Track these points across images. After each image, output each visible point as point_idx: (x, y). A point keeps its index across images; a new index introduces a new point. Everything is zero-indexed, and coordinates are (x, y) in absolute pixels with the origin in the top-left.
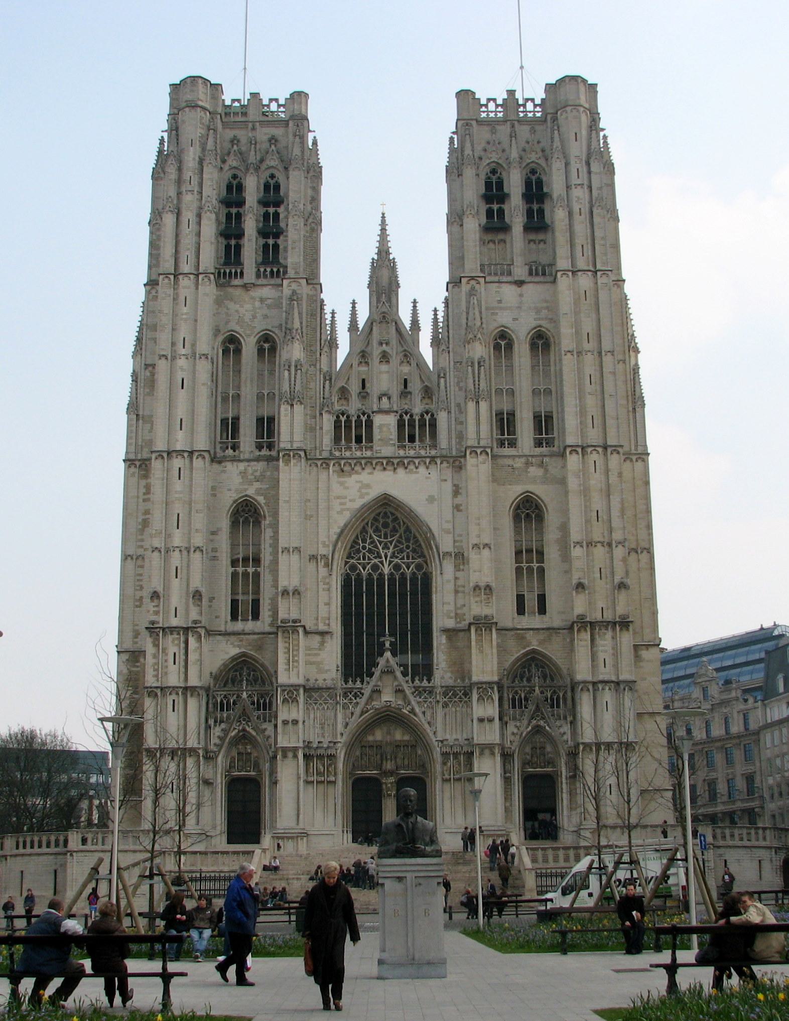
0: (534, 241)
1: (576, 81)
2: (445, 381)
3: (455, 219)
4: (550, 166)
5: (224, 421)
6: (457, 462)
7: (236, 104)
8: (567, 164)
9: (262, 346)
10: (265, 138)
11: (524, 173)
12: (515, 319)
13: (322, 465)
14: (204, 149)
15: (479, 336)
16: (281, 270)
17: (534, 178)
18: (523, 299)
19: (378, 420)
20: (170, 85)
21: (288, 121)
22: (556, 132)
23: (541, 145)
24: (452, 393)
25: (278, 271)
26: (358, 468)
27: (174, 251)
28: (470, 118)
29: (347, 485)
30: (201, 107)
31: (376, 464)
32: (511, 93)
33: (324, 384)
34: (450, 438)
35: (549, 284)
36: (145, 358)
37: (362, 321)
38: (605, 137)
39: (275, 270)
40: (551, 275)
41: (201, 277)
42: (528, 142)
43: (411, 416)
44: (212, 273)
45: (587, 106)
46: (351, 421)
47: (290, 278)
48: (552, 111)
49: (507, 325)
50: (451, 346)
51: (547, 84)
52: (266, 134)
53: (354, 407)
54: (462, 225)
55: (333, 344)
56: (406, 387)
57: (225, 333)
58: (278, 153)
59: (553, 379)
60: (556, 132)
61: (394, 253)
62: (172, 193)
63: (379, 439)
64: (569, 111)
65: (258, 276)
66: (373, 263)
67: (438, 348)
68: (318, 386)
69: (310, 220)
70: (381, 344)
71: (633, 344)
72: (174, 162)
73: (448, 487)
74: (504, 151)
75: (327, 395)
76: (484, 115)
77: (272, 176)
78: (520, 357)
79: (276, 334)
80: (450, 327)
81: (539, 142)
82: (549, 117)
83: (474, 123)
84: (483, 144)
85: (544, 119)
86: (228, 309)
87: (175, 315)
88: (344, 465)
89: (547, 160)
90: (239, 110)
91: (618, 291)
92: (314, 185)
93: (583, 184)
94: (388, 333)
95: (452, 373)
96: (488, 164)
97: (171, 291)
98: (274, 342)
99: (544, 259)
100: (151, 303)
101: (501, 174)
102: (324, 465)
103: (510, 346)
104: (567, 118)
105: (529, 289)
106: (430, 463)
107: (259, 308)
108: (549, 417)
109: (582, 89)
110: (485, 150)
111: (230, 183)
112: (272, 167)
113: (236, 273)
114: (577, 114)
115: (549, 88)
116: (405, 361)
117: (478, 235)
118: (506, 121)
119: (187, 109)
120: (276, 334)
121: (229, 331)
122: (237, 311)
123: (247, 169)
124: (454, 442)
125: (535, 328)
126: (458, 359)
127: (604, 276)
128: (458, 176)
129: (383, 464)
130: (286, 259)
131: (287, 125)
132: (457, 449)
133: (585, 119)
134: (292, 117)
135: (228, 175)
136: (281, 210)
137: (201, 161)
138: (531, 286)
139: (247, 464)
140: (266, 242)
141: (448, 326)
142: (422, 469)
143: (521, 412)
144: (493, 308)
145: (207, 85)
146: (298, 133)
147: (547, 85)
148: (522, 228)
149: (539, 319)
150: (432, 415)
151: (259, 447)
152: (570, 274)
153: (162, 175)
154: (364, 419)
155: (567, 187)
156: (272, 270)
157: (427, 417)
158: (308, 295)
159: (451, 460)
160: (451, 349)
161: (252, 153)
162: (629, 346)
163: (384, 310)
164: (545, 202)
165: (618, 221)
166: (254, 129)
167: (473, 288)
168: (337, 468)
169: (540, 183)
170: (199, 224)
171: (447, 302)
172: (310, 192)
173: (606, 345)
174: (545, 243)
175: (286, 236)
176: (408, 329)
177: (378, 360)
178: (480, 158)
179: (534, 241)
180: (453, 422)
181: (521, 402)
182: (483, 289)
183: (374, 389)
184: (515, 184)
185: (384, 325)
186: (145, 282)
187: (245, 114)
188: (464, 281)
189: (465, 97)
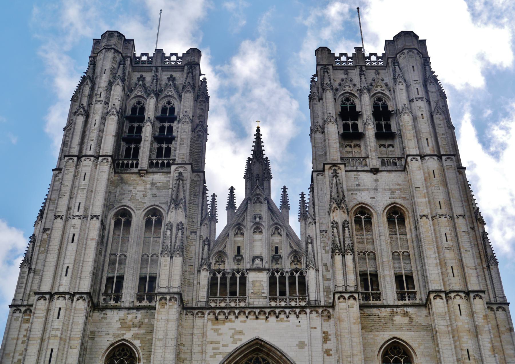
0: (384, 146)
7: (144, 58)
9: (150, 219)
11: (372, 99)
13: (197, 314)
15: (343, 205)
18: (378, 183)
19: (251, 277)
22: (397, 67)
23: (385, 82)
24: (319, 254)
26: (232, 317)
27: (80, 141)
29: (220, 332)
31: (249, 313)
33: (203, 247)
34: (318, 292)
35: (400, 173)
36: (45, 224)
41: (100, 159)
43: (282, 274)
44: (110, 156)
46: (226, 278)
47: (177, 164)
49: (365, 202)
52: (166, 75)
53: (229, 265)
54: (323, 132)
55: (213, 218)
57: (118, 207)
58: (174, 87)
59: (410, 244)
60: (397, 67)
63: (253, 293)
65: (151, 165)
67: (306, 222)
68: (197, 248)
69: (198, 129)
70: (255, 218)
71: (479, 217)
73: (318, 334)
74: (355, 85)
75: (205, 257)
76: (338, 64)
79: (163, 209)
80: (316, 204)
82: (390, 60)
83: (331, 67)
84: (338, 81)
86: (123, 190)
87: (73, 187)
88: (219, 314)
89: (390, 90)
91: (461, 177)
92: (202, 107)
94: (261, 211)
95: (318, 239)
96: (343, 94)
97: (73, 169)
98: (161, 215)
101: (353, 101)
102: (200, 314)
103: (369, 221)
105: (383, 176)
106: (300, 313)
107: (151, 189)
111: (135, 106)
112: (170, 96)
116: (276, 232)
118: (356, 66)
119: (104, 51)
120: (163, 209)
121: (121, 206)
122: (131, 191)
123: (149, 95)
124: (322, 295)
126: (324, 228)
128: (319, 101)
129: (255, 313)
131: (183, 70)
132: (325, 301)
135: (132, 102)
136: (175, 125)
138: (385, 173)
139: (127, 312)
140: (161, 146)
141: (314, 204)
142: (293, 317)
143: (383, 269)
144: (352, 190)
145: (121, 38)
147: (386, 41)
150: (301, 273)
151: (140, 298)
157: (297, 275)
159: (320, 310)
160: (317, 220)
163: (258, 191)
165: (454, 128)
166: (157, 71)
167: (335, 171)
168: (212, 316)
172: (199, 112)
174: (393, 147)
176: (279, 208)
177: (252, 231)
179: (382, 145)
180: (321, 278)
181: (383, 263)
182: (344, 176)
185: (258, 205)
186: (55, 167)
187: (151, 62)
188: (327, 167)
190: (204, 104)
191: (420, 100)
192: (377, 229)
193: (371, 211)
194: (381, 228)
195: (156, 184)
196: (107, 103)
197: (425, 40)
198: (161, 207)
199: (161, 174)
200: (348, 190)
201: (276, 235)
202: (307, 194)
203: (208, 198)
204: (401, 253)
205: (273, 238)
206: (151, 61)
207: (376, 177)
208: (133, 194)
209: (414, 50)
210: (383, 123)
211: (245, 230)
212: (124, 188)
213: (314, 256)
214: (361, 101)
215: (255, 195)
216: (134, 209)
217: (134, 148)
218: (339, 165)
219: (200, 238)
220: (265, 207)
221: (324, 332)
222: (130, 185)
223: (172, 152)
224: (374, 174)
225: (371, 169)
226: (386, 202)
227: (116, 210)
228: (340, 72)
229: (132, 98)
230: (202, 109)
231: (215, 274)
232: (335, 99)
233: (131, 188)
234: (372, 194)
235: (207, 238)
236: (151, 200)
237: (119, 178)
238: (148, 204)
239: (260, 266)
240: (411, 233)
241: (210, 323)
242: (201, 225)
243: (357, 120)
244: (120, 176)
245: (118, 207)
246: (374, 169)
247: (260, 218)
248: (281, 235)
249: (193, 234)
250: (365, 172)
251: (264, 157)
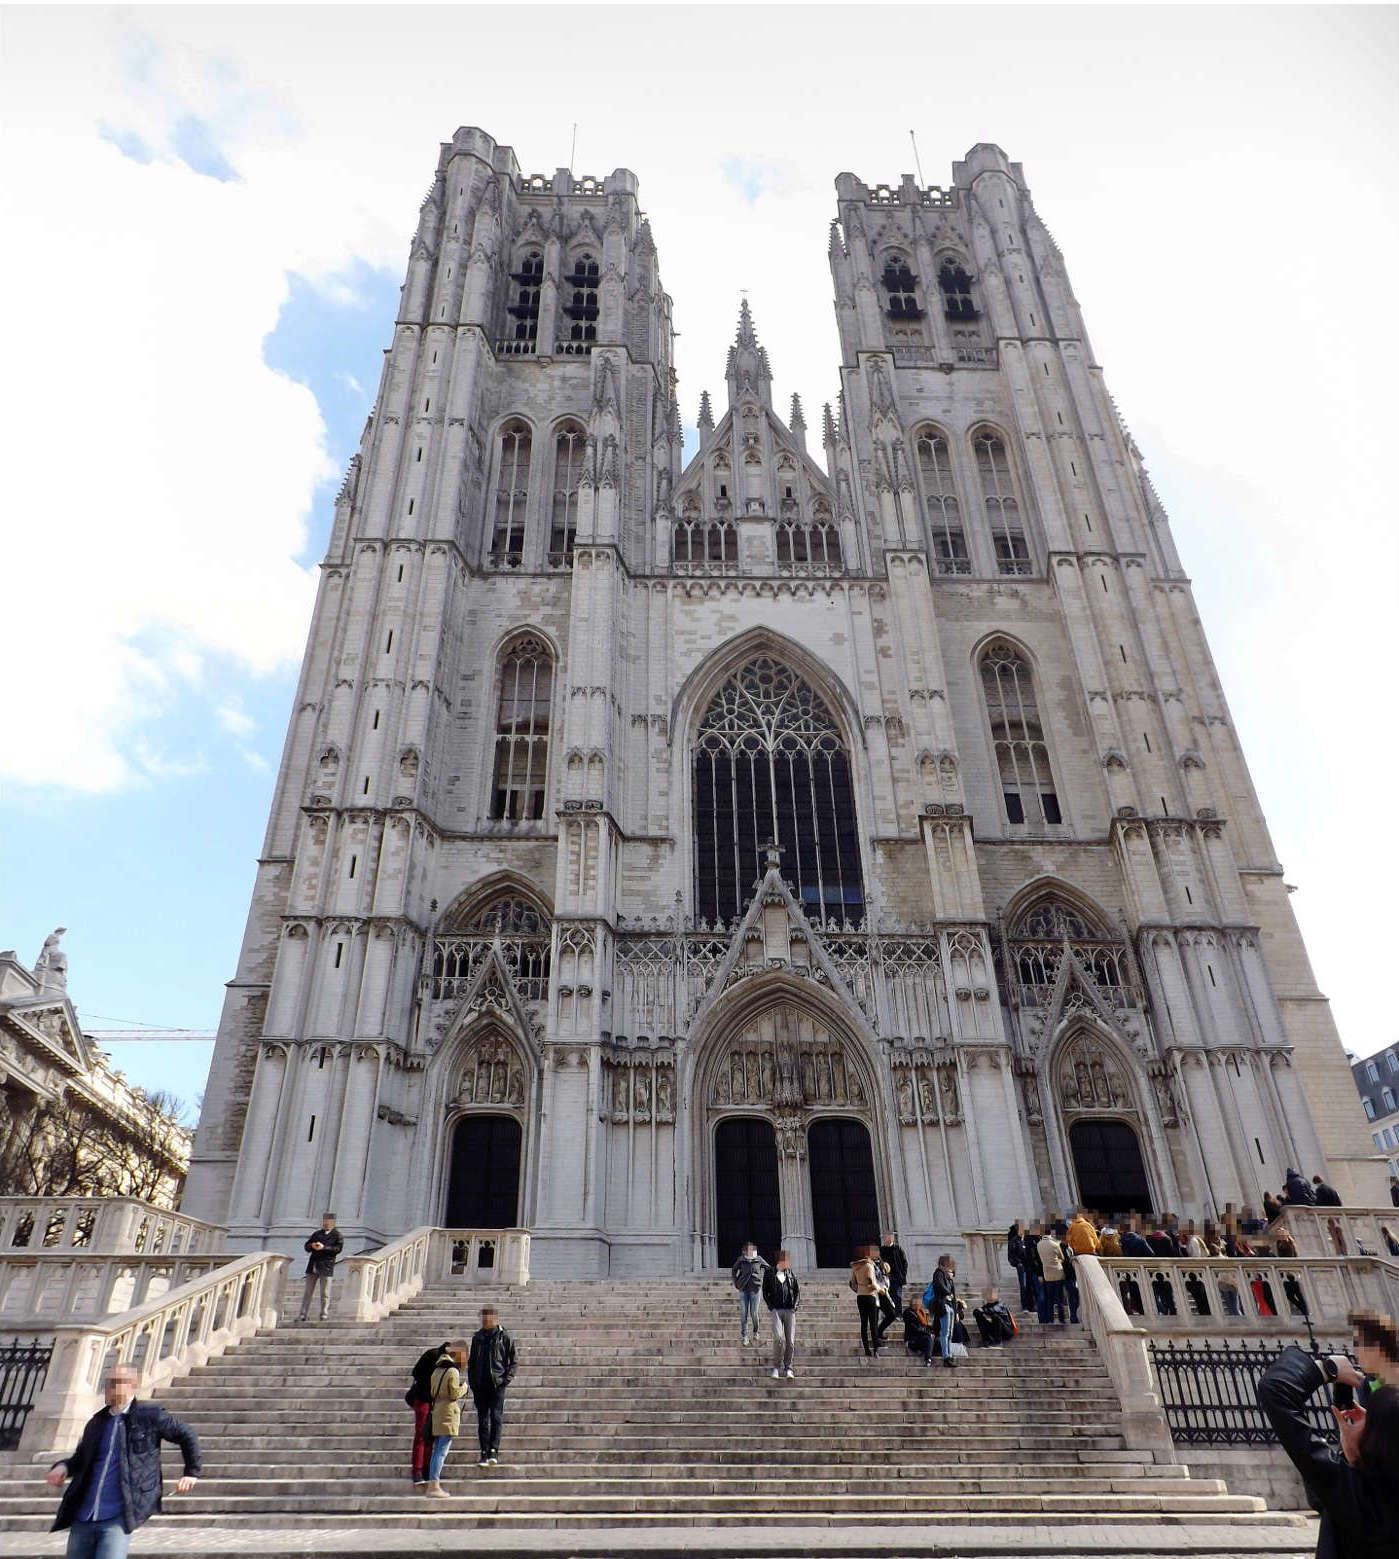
3: (845, 302)
5: (500, 533)
6: (877, 585)
7: (538, 183)
10: (577, 215)
12: (945, 411)
13: (654, 586)
19: (745, 531)
21: (607, 197)
24: (860, 498)
26: (714, 592)
29: (696, 615)
31: (744, 588)
32: (908, 178)
34: (861, 556)
43: (798, 527)
46: (702, 532)
53: (708, 513)
55: (673, 437)
59: (1016, 486)
61: (762, 340)
63: (748, 557)
65: (560, 350)
69: (637, 298)
73: (865, 622)
74: (906, 236)
83: (862, 204)
84: (876, 229)
88: (692, 587)
89: (967, 246)
103: (942, 448)
106: (832, 588)
122: (526, 390)
129: (754, 588)
138: (964, 372)
141: (846, 420)
142: (820, 596)
143: (971, 524)
149: (982, 412)
150: (831, 527)
154: (722, 529)
157: (823, 530)
159: (867, 585)
163: (748, 398)
166: (560, 203)
168: (679, 591)
171: (842, 397)
172: (638, 270)
177: (743, 459)
178: (875, 242)
179: (960, 332)
180: (865, 536)
181: (969, 513)
183: (736, 496)
184: (924, 266)
189: (845, 181)
194: (965, 459)
206: (550, 189)
214: (916, 259)
215: (745, 404)
220: (763, 421)
221: (876, 620)
222: (524, 381)
225: (941, 365)
228: (879, 214)
230: (644, 267)
232: (871, 255)
233: (527, 385)
235: (665, 469)
237: (504, 370)
238: (560, 412)
239: (759, 513)
241: (677, 602)
247: (756, 440)
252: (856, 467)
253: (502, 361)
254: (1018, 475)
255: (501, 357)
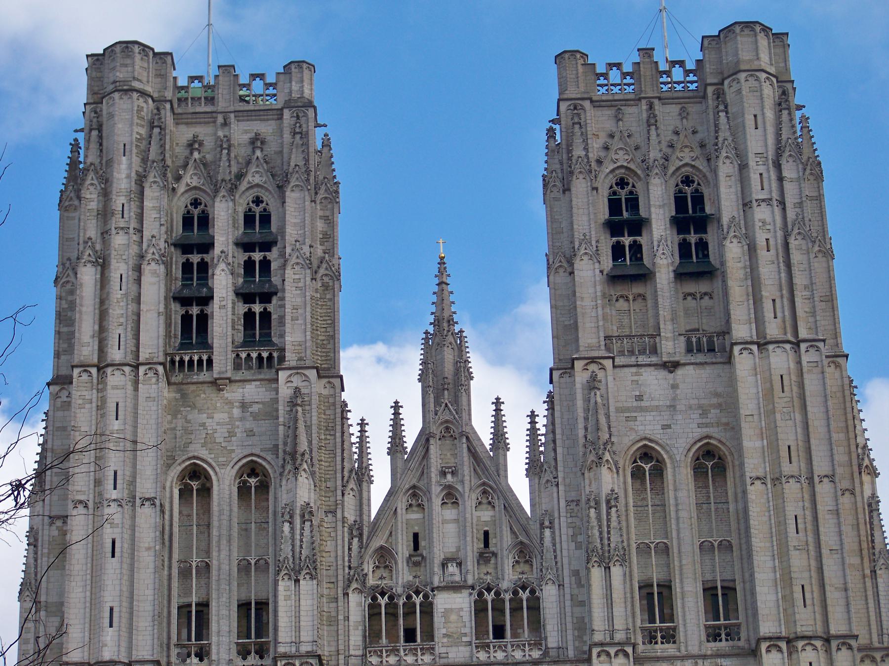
1: (753, 30)
2: (553, 533)
4: (715, 172)
8: (743, 167)
9: (245, 482)
10: (246, 137)
11: (672, 182)
14: (145, 160)
15: (607, 456)
16: (275, 355)
17: (688, 190)
18: (678, 392)
19: (442, 602)
20: (88, 56)
21: (282, 109)
22: (722, 114)
23: (699, 136)
24: (565, 553)
25: (270, 357)
27: (97, 327)
28: (579, 96)
30: (137, 91)
32: (647, 52)
33: (350, 544)
34: (563, 631)
35: (720, 366)
37: (411, 435)
38: (805, 119)
39: (265, 355)
40: (723, 349)
41: (142, 369)
42: (677, 133)
43: (498, 594)
44: (160, 364)
45: (772, 70)
46: (396, 606)
47: (290, 369)
48: (715, 81)
49: (652, 437)
50: (561, 475)
51: (703, 37)
52: (246, 132)
54: (572, 273)
56: (486, 544)
57: (184, 461)
60: (722, 114)
62: (92, 231)
63: (445, 635)
64: (742, 79)
65: (237, 366)
66: (426, 339)
68: (340, 548)
69: (322, 271)
70: (443, 474)
71: (866, 462)
72: (95, 182)
77: (258, 201)
78: (675, 490)
79: (269, 463)
80: (558, 442)
81: (694, 132)
82: (710, 90)
83: (587, 104)
84: (603, 139)
85: (702, 94)
86: (188, 422)
89: (709, 160)
90: (199, 93)
93: (771, 199)
96: (612, 171)
98: (266, 474)
99: (711, 325)
100: (60, 414)
101: (634, 186)
103: (659, 472)
104: (739, 91)
105: (686, 374)
107: (242, 419)
108: (729, 590)
109: (763, 42)
110: (607, 148)
112: (258, 185)
113: (200, 361)
114: (756, 84)
115: (710, 42)
116: (485, 501)
117: (599, 288)
118: (640, 99)
119: (116, 95)
120: (269, 463)
121: (189, 459)
122: (203, 425)
123: (216, 191)
124: (570, 637)
125: (700, 440)
126: (573, 495)
127: (812, 350)
128: (564, 192)
130: (282, 336)
131: (280, 117)
132: (576, 648)
133: (769, 92)
134: (289, 105)
135: (181, 203)
136: (273, 255)
137: (141, 180)
138: (691, 367)
141: (554, 441)
144: (628, 409)
145: (147, 55)
146: (298, 130)
148: (672, 275)
149: (707, 425)
150: (533, 592)
152: (755, 348)
153: (76, 202)
154: (418, 600)
155: (745, 205)
156: (260, 355)
157: (524, 595)
158: (320, 395)
160: (560, 480)
161: (224, 163)
162: (860, 466)
164: (709, 229)
166: (226, 124)
167: (594, 378)
169: (699, 199)
170: (138, 281)
172: (320, 225)
173: (821, 466)
174: (711, 298)
175: (283, 299)
176: (488, 447)
177: (440, 502)
178: (599, 162)
179: (690, 294)
180: (568, 603)
181: (681, 566)
186: (49, 379)
187: (211, 100)
188: (579, 365)
190: (329, 206)
191: (763, 204)
192: (671, 494)
193: (662, 456)
194: (682, 494)
195: (251, 406)
196: (140, 231)
197: (787, 34)
198: (265, 459)
199: (258, 383)
200: (619, 410)
201: (484, 506)
202: (541, 416)
203: (352, 430)
204: (716, 544)
205: (478, 513)
207: (674, 379)
208: (209, 432)
209: (757, 73)
210: (693, 241)
211: (425, 499)
212: (190, 417)
213: (555, 557)
215: (442, 423)
216: (214, 464)
217: (197, 315)
218: (601, 361)
219: (343, 522)
223: (274, 323)
224: (671, 372)
225: (665, 362)
226: (690, 435)
227: (180, 468)
229: (182, 194)
231: (374, 598)
234: (666, 417)
236: (245, 444)
237: (178, 396)
238: (239, 453)
239: (457, 578)
240: (736, 501)
242: (343, 495)
243: (640, 235)
244: (179, 391)
245: (184, 461)
246: (669, 362)
248: (494, 507)
249: (330, 515)
250: (653, 368)
251: (457, 329)
252: (563, 510)
253: (175, 384)
254: (737, 510)
255: (173, 379)
